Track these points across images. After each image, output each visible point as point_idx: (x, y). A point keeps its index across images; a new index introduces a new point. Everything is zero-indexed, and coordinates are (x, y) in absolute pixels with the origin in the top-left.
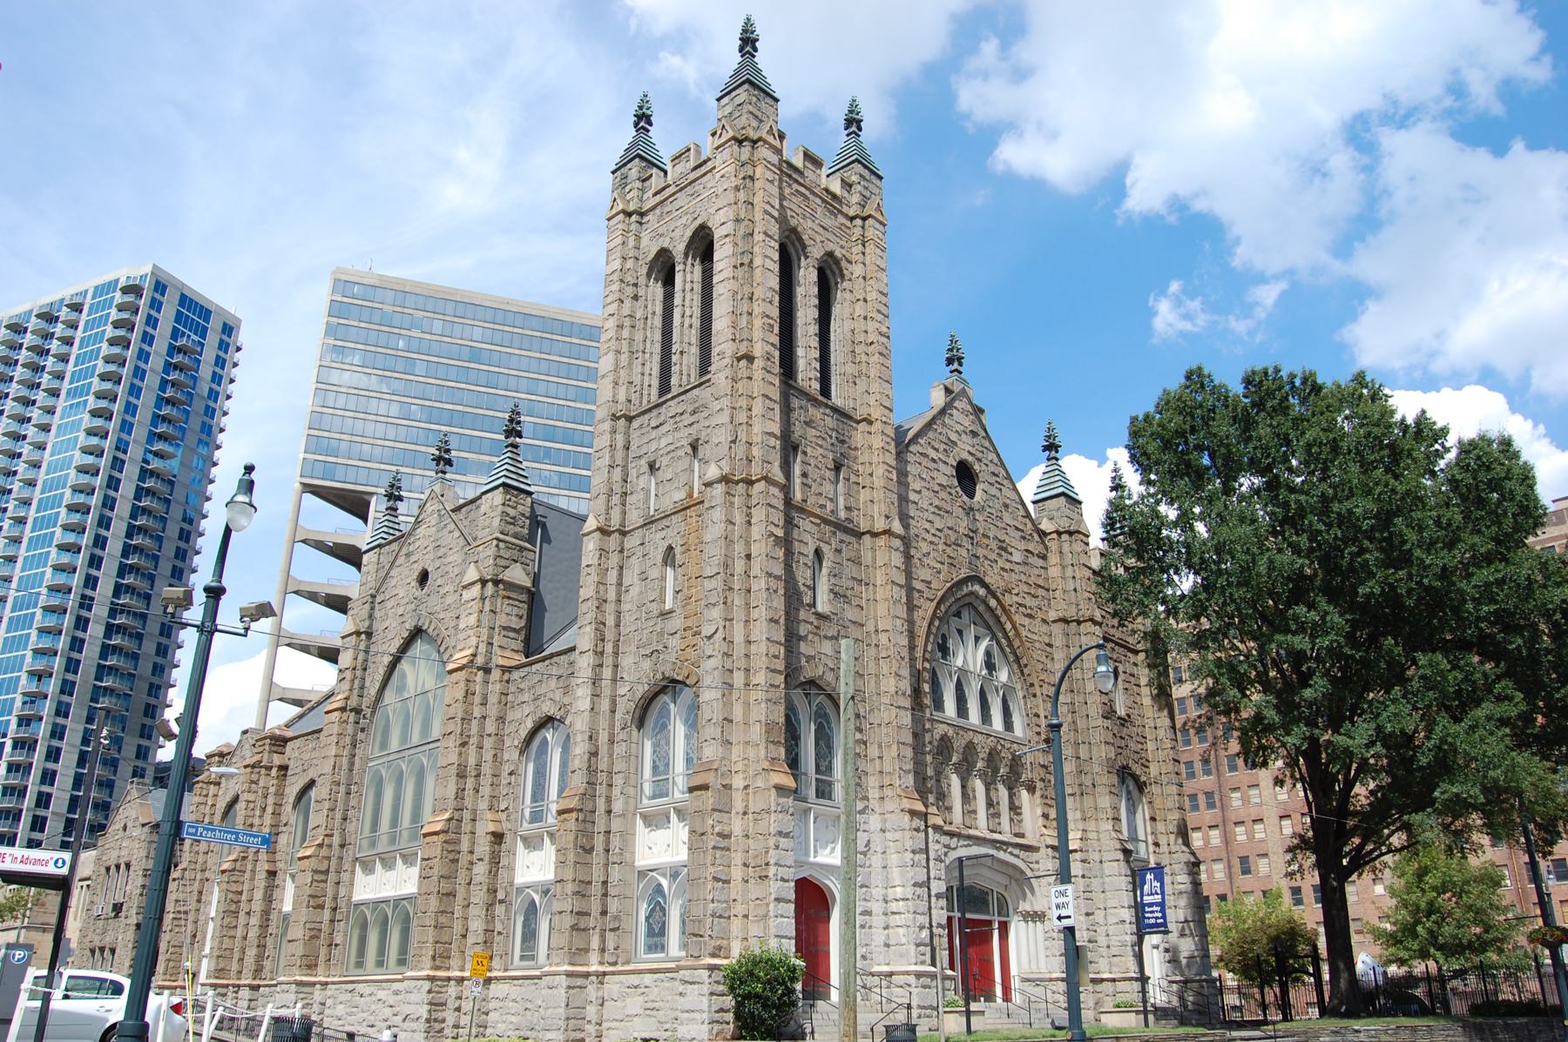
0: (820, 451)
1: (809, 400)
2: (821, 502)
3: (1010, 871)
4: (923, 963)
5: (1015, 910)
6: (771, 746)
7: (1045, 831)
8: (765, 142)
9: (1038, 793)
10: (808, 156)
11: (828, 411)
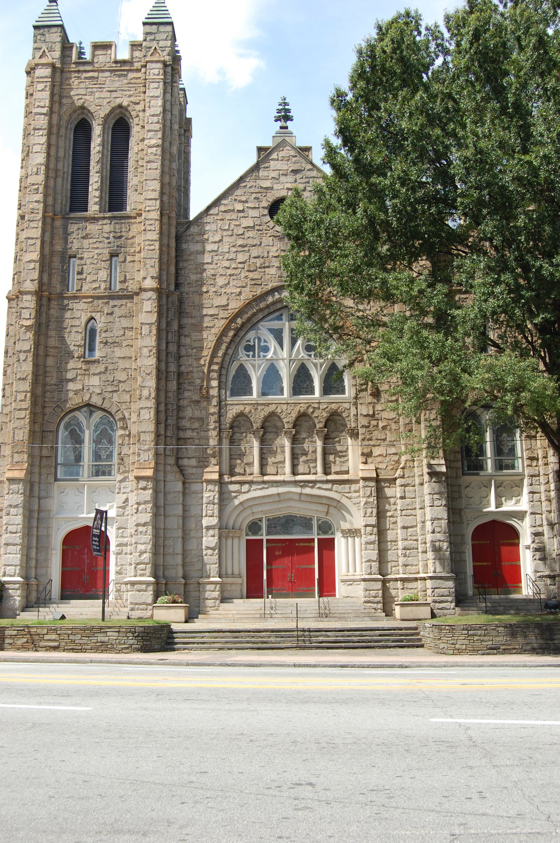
0: (97, 251)
1: (86, 221)
2: (96, 285)
3: (324, 501)
4: (141, 575)
5: (337, 529)
6: (16, 455)
7: (362, 466)
8: (37, 65)
9: (361, 437)
10: (96, 47)
11: (105, 222)
